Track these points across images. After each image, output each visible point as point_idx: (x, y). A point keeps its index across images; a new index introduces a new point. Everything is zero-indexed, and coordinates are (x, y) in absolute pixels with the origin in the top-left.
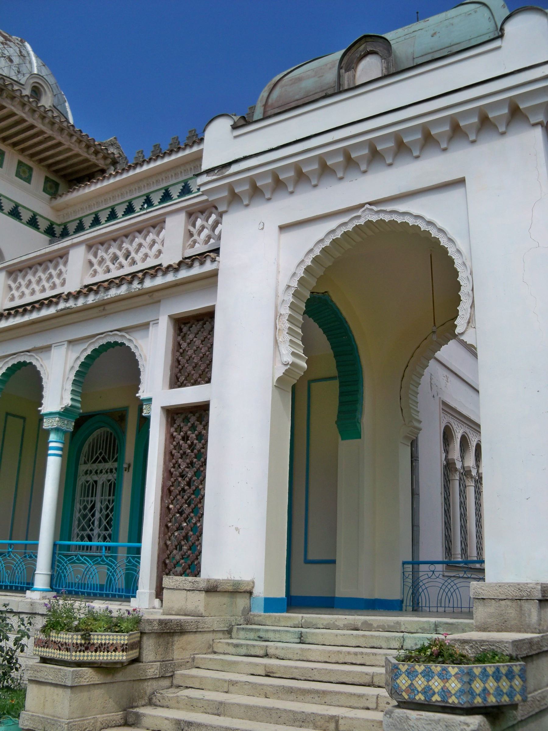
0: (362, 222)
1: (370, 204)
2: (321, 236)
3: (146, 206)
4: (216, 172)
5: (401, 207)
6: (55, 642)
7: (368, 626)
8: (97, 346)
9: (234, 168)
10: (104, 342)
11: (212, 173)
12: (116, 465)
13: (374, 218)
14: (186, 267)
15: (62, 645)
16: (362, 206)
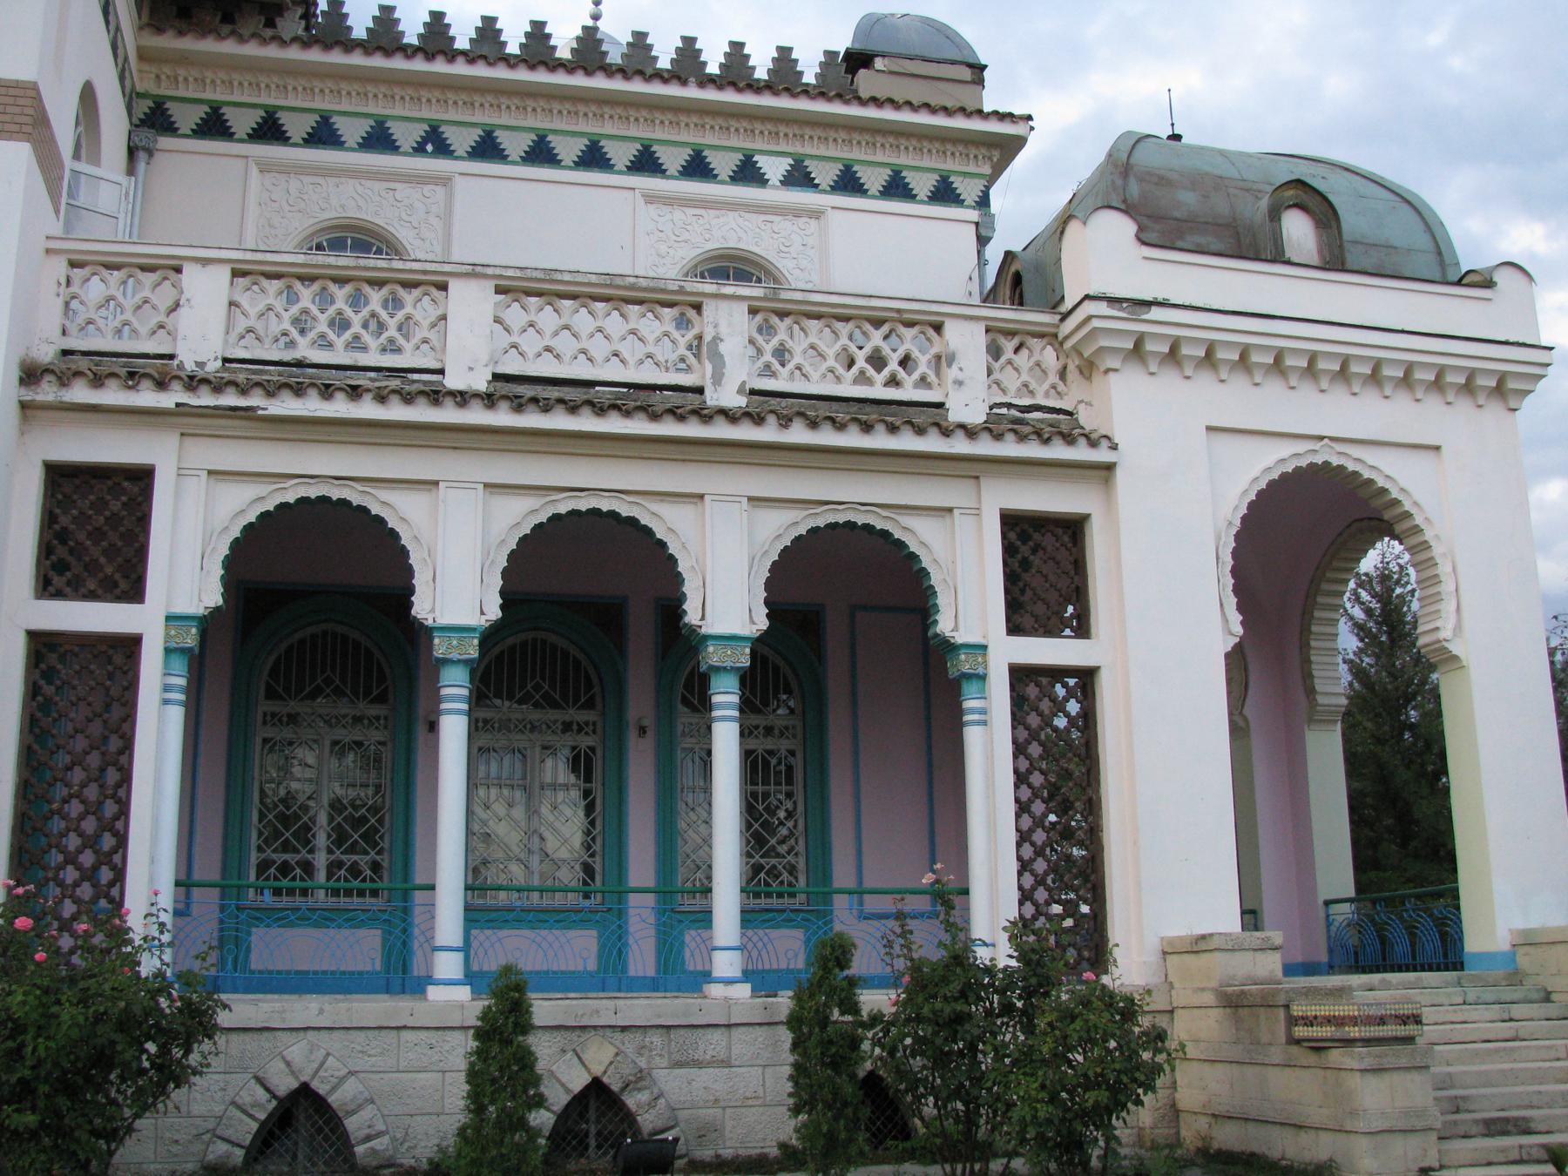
0: (1319, 460)
1: (1332, 439)
2: (1270, 460)
3: (429, 148)
4: (1125, 305)
5: (1371, 456)
6: (1396, 1016)
7: (1387, 986)
8: (821, 522)
9: (1156, 313)
10: (841, 518)
11: (1117, 305)
12: (374, 710)
13: (1335, 461)
14: (1061, 442)
15: (1408, 1017)
16: (1321, 438)
